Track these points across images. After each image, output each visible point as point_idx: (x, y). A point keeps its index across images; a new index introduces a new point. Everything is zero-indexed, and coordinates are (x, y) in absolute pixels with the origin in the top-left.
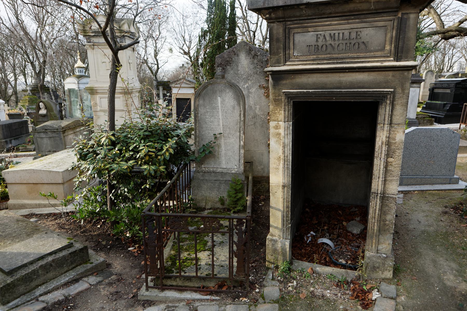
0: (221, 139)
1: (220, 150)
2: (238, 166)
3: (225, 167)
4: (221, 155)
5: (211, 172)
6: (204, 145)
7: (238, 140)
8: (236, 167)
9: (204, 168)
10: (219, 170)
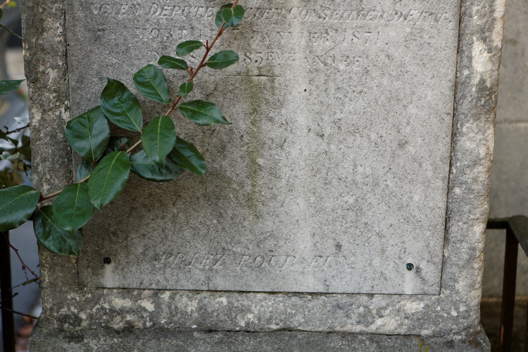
0: (282, 21)
1: (271, 131)
2: (430, 272)
3: (310, 284)
4: (274, 173)
5: (181, 331)
6: (114, 88)
7: (449, 29)
8: (409, 283)
9: (125, 291)
10: (258, 311)
